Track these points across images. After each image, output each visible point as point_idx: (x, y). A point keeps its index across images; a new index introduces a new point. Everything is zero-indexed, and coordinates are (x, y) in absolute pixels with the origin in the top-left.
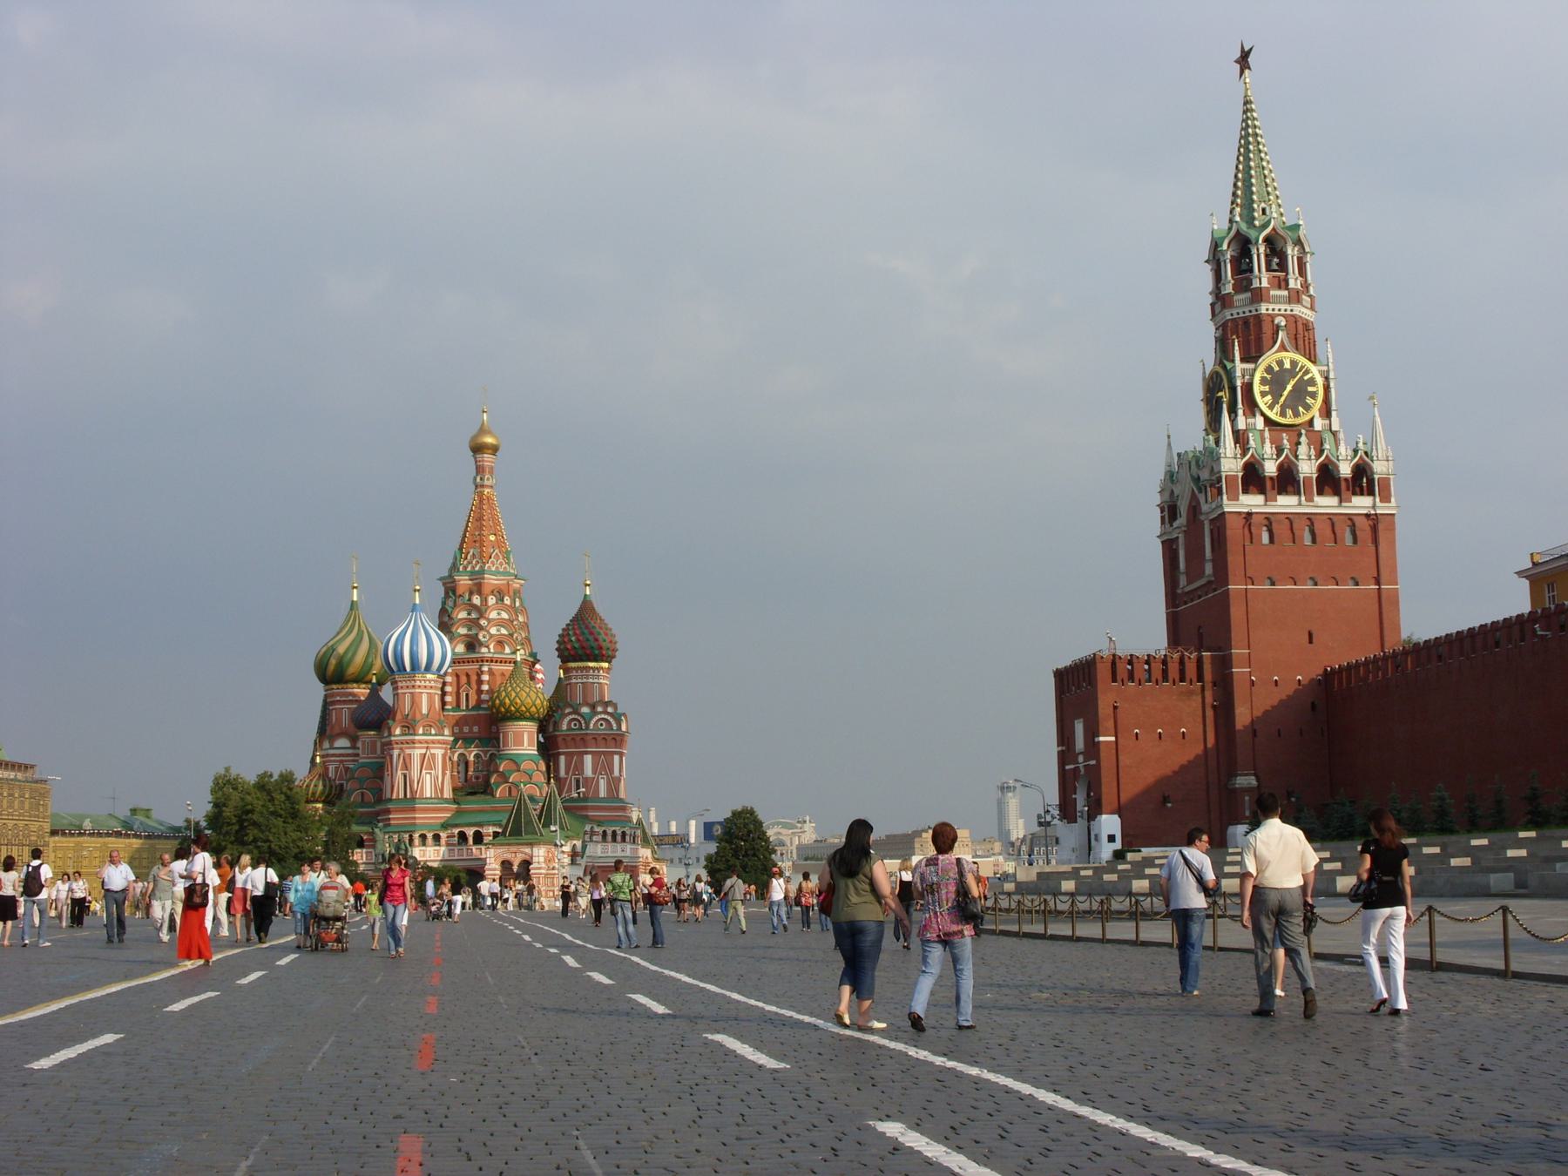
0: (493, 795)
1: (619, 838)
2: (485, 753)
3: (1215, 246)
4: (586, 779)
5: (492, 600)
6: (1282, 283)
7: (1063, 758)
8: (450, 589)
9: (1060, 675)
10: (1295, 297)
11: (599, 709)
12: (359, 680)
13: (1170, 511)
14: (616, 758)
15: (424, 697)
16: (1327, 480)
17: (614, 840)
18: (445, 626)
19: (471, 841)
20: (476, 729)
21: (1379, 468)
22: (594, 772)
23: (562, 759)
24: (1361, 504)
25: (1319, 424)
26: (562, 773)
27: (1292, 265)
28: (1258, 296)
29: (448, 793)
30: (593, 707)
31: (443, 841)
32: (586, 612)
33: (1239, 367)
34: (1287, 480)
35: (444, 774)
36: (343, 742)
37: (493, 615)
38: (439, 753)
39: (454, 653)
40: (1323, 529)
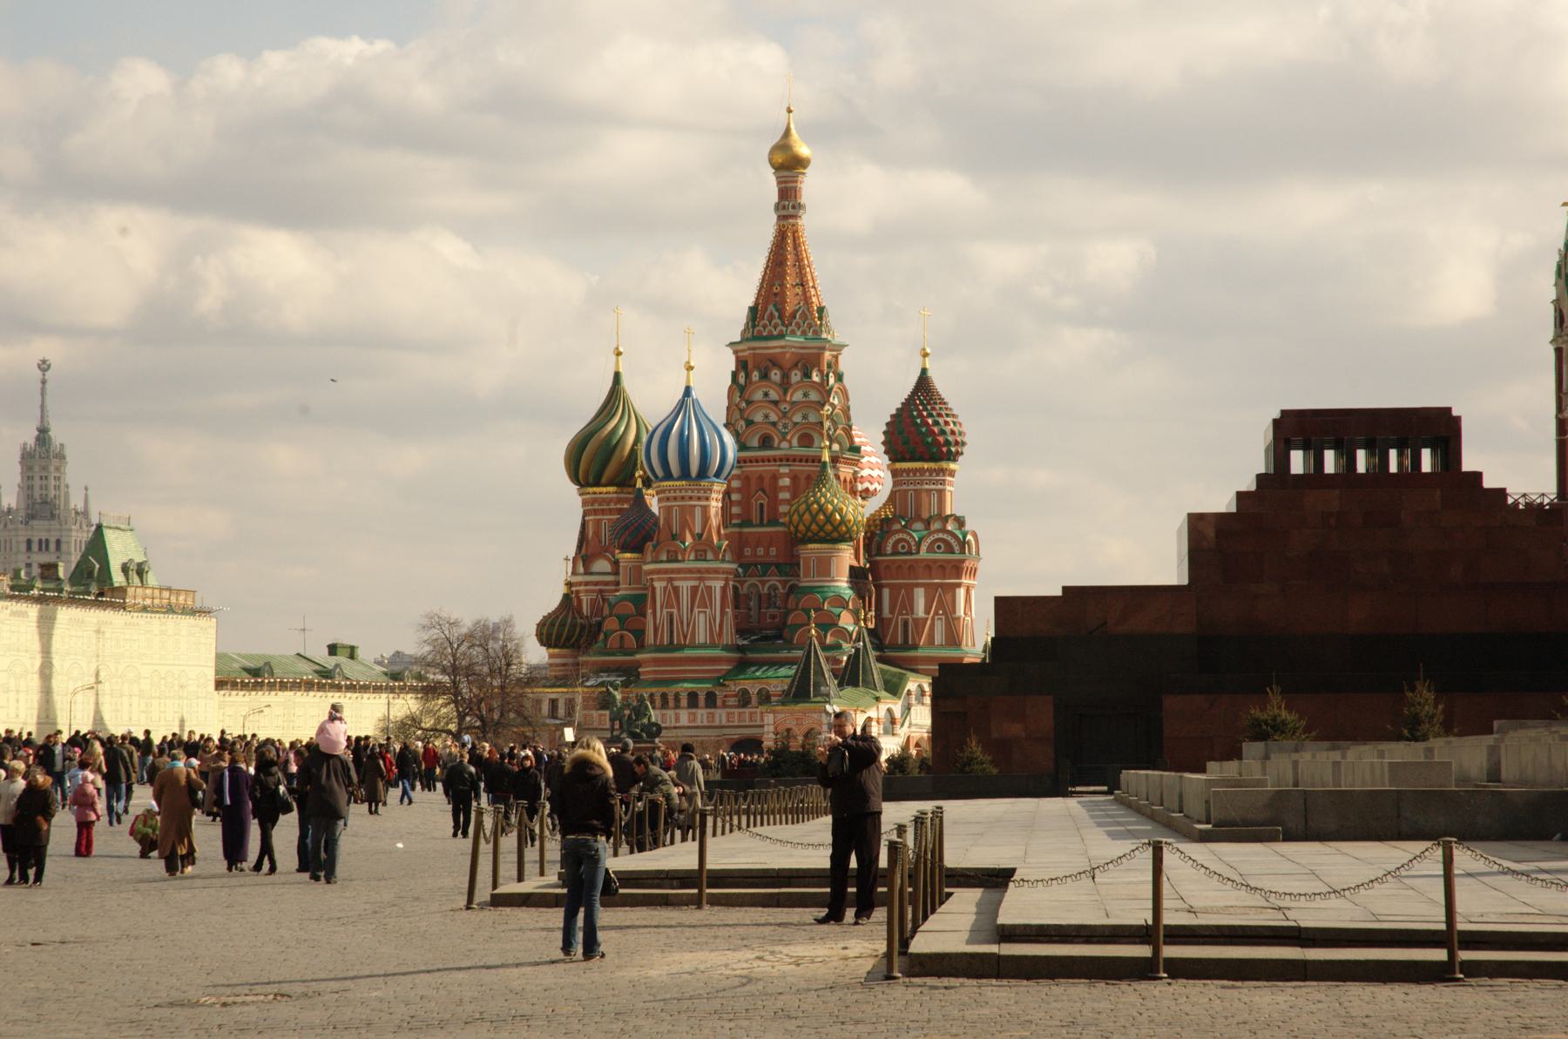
2: (784, 583)
4: (916, 621)
5: (796, 376)
11: (936, 525)
14: (961, 592)
19: (754, 700)
20: (773, 551)
22: (927, 611)
23: (886, 592)
26: (886, 613)
29: (729, 637)
30: (928, 523)
31: (719, 702)
35: (723, 613)
36: (602, 565)
37: (798, 396)
38: (717, 585)
39: (742, 446)
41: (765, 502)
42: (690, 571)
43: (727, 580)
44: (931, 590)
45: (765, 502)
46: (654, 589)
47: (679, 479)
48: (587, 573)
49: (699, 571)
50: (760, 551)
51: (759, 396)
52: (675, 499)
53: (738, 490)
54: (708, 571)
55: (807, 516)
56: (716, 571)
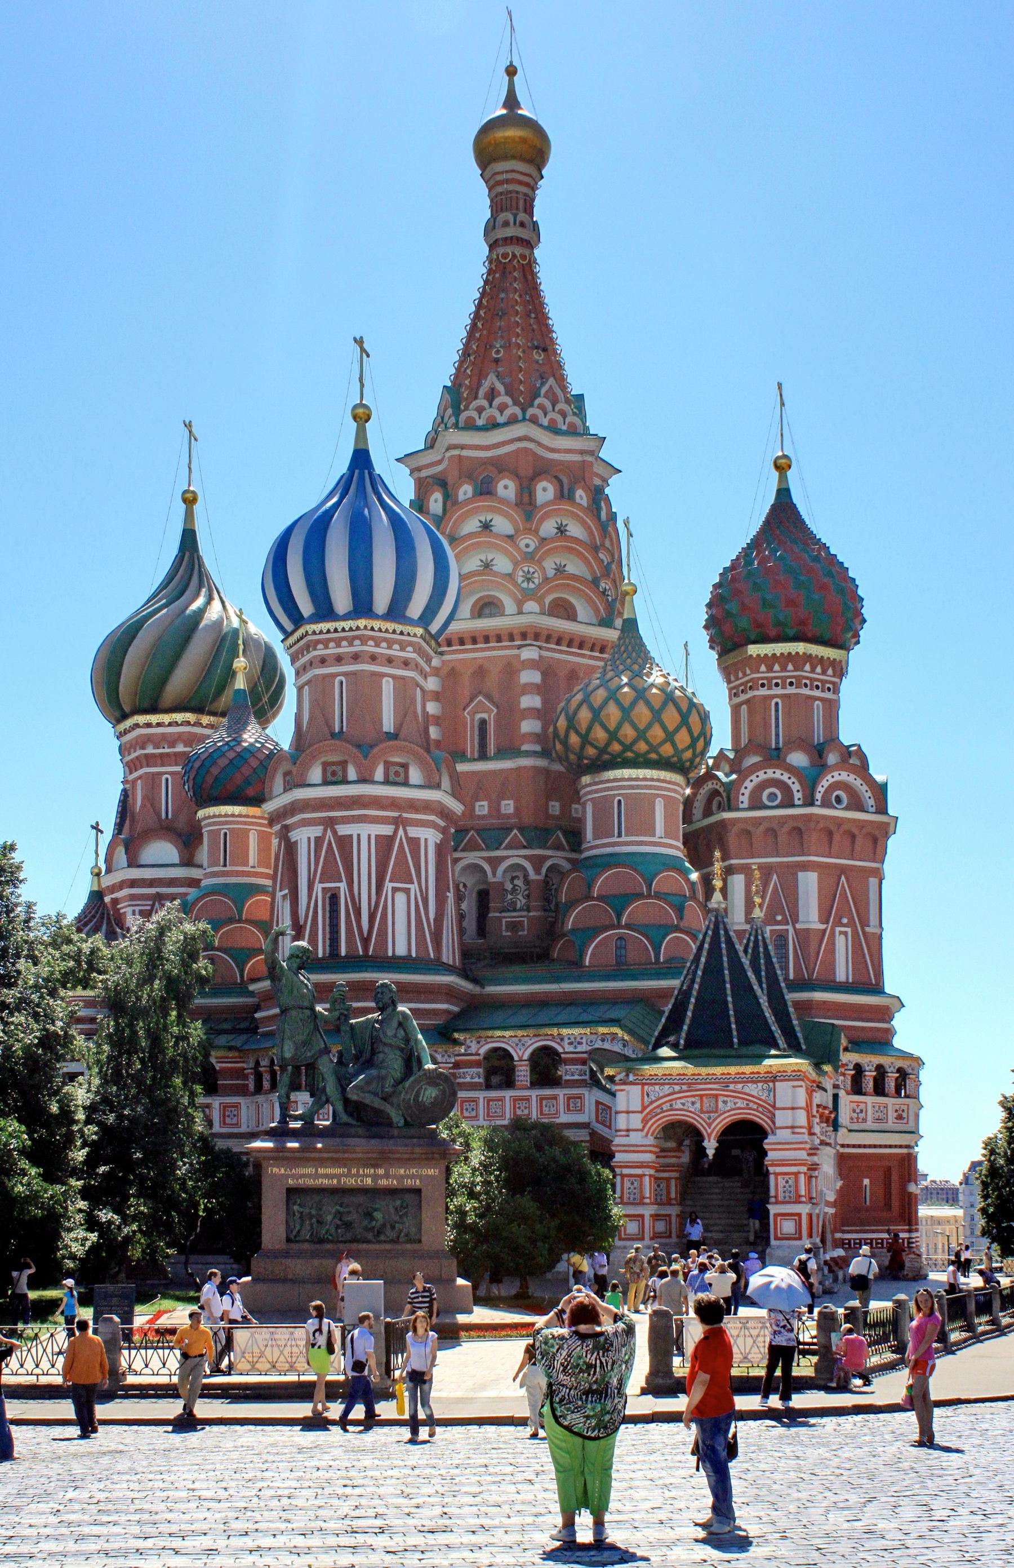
0: (577, 963)
1: (890, 1084)
2: (537, 862)
14: (873, 881)
15: (387, 687)
17: (879, 1090)
20: (508, 806)
29: (449, 954)
38: (430, 837)
41: (490, 716)
42: (376, 802)
43: (444, 831)
44: (830, 875)
45: (490, 716)
46: (291, 849)
47: (346, 617)
48: (133, 863)
49: (393, 804)
50: (482, 808)
51: (472, 525)
52: (339, 659)
53: (436, 696)
54: (413, 805)
55: (613, 712)
56: (426, 807)
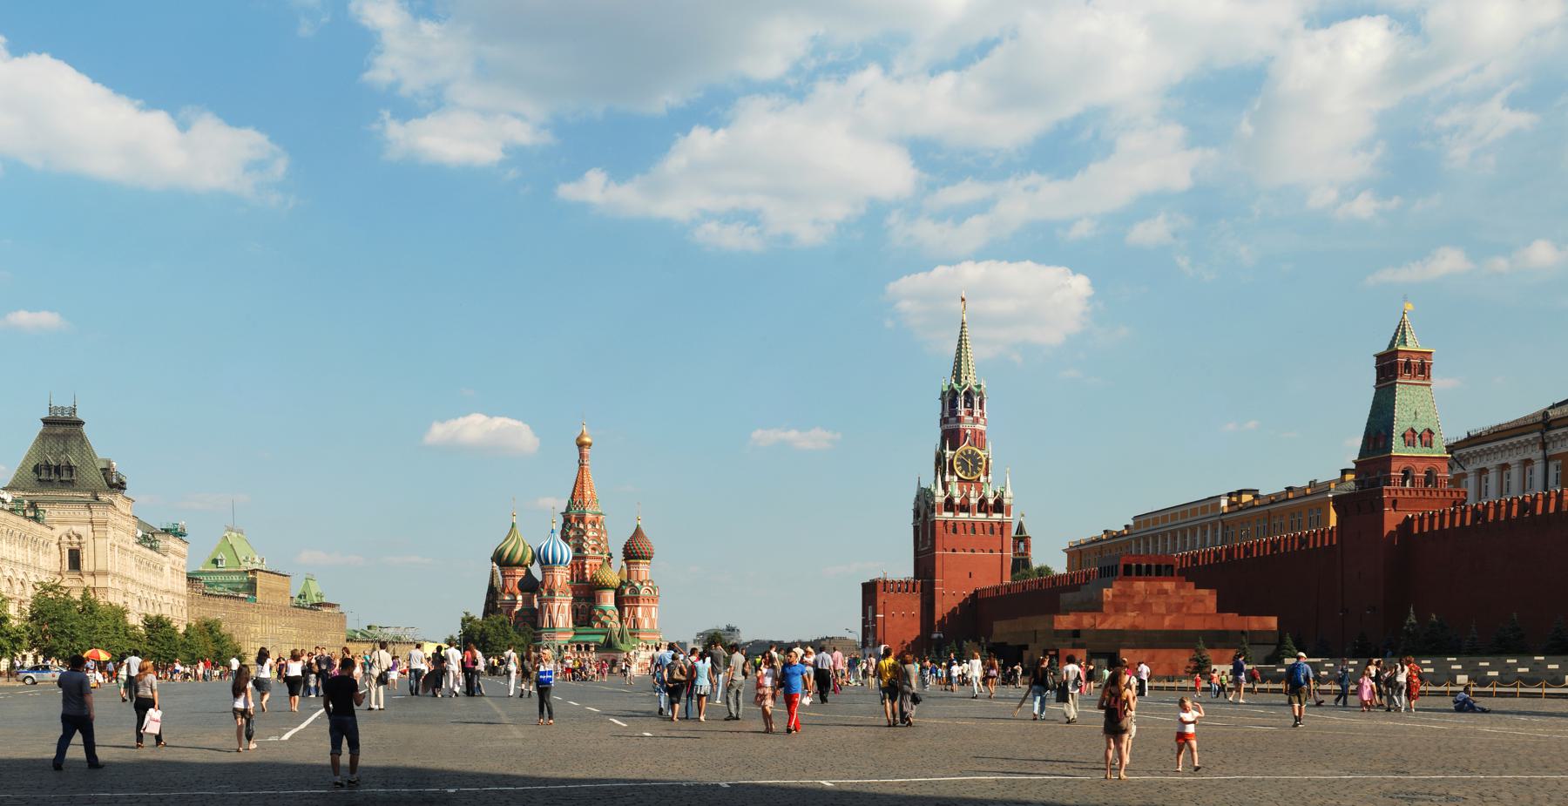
3: (943, 393)
6: (971, 414)
7: (865, 622)
8: (567, 520)
9: (864, 585)
10: (976, 421)
12: (519, 565)
13: (917, 513)
16: (983, 506)
18: (565, 538)
21: (1006, 501)
24: (997, 516)
25: (982, 479)
27: (977, 405)
28: (959, 420)
32: (638, 532)
33: (948, 453)
34: (964, 508)
40: (979, 528)
